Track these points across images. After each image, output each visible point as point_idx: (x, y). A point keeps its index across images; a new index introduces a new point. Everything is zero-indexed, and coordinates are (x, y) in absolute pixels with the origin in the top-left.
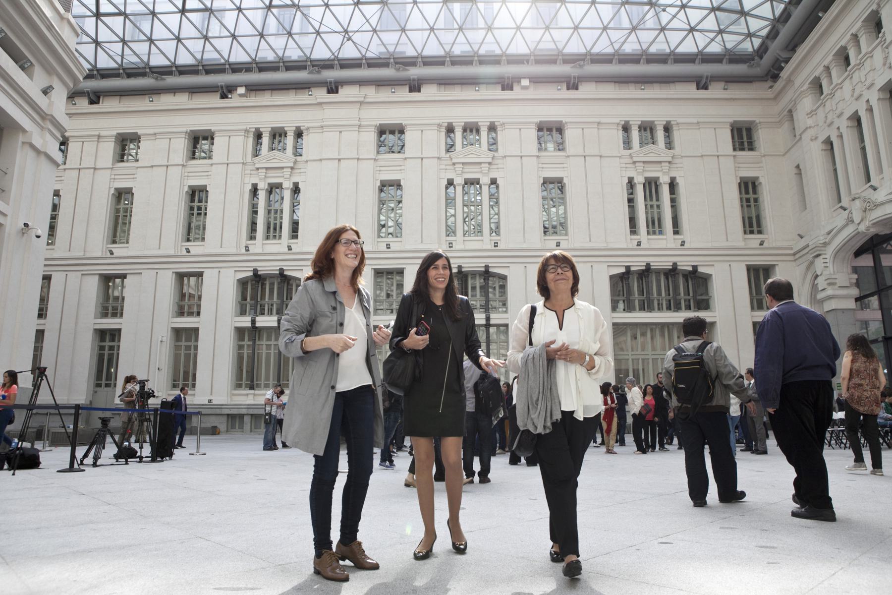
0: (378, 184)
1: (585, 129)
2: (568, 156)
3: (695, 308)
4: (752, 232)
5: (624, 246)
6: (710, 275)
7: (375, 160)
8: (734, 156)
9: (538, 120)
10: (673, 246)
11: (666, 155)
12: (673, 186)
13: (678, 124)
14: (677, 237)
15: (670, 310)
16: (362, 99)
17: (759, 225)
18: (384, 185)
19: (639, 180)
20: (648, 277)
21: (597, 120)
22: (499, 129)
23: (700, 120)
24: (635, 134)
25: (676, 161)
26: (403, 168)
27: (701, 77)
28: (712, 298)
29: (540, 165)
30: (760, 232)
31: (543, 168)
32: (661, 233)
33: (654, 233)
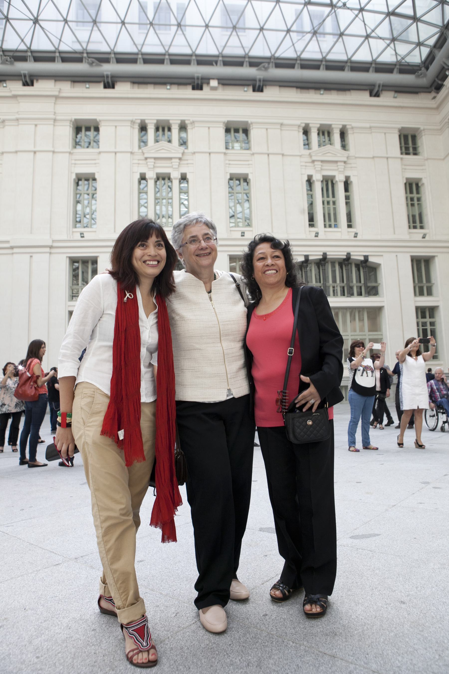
0: (74, 176)
1: (269, 130)
2: (253, 154)
3: (365, 293)
4: (415, 227)
5: (304, 237)
6: (379, 265)
7: (70, 153)
8: (402, 159)
9: (226, 120)
10: (347, 237)
11: (341, 155)
12: (347, 185)
13: (352, 128)
14: (350, 230)
15: (344, 295)
16: (56, 93)
17: (421, 221)
18: (79, 179)
19: (317, 178)
20: (325, 265)
21: (281, 121)
22: (189, 127)
23: (373, 125)
24: (314, 135)
25: (350, 161)
26: (97, 161)
27: (374, 85)
28: (380, 285)
29: (227, 162)
30: (422, 228)
31: (229, 164)
32: (336, 226)
33: (330, 226)
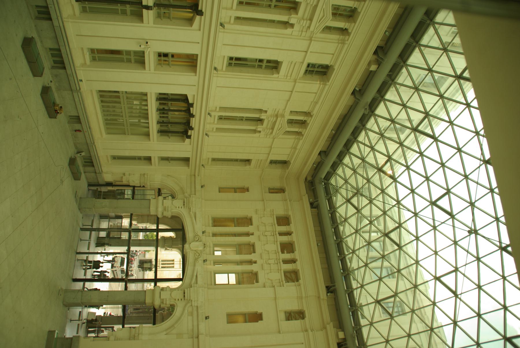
19: (263, 116)
23: (297, 151)
